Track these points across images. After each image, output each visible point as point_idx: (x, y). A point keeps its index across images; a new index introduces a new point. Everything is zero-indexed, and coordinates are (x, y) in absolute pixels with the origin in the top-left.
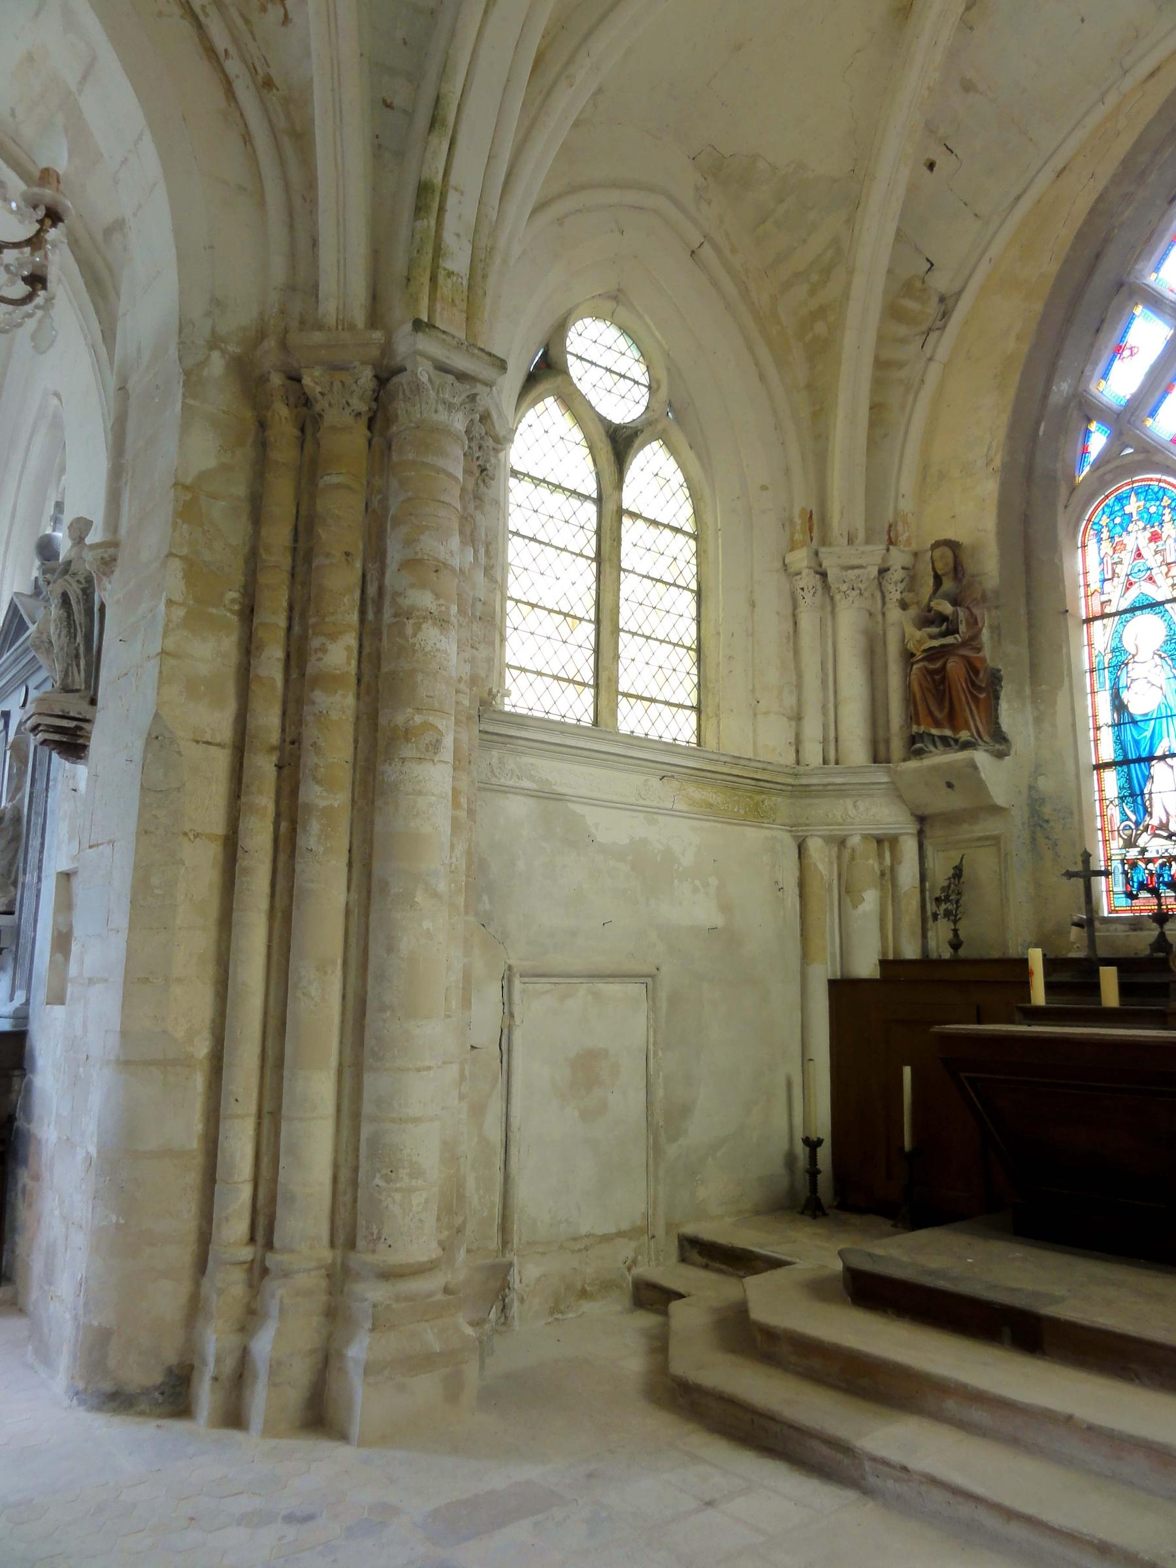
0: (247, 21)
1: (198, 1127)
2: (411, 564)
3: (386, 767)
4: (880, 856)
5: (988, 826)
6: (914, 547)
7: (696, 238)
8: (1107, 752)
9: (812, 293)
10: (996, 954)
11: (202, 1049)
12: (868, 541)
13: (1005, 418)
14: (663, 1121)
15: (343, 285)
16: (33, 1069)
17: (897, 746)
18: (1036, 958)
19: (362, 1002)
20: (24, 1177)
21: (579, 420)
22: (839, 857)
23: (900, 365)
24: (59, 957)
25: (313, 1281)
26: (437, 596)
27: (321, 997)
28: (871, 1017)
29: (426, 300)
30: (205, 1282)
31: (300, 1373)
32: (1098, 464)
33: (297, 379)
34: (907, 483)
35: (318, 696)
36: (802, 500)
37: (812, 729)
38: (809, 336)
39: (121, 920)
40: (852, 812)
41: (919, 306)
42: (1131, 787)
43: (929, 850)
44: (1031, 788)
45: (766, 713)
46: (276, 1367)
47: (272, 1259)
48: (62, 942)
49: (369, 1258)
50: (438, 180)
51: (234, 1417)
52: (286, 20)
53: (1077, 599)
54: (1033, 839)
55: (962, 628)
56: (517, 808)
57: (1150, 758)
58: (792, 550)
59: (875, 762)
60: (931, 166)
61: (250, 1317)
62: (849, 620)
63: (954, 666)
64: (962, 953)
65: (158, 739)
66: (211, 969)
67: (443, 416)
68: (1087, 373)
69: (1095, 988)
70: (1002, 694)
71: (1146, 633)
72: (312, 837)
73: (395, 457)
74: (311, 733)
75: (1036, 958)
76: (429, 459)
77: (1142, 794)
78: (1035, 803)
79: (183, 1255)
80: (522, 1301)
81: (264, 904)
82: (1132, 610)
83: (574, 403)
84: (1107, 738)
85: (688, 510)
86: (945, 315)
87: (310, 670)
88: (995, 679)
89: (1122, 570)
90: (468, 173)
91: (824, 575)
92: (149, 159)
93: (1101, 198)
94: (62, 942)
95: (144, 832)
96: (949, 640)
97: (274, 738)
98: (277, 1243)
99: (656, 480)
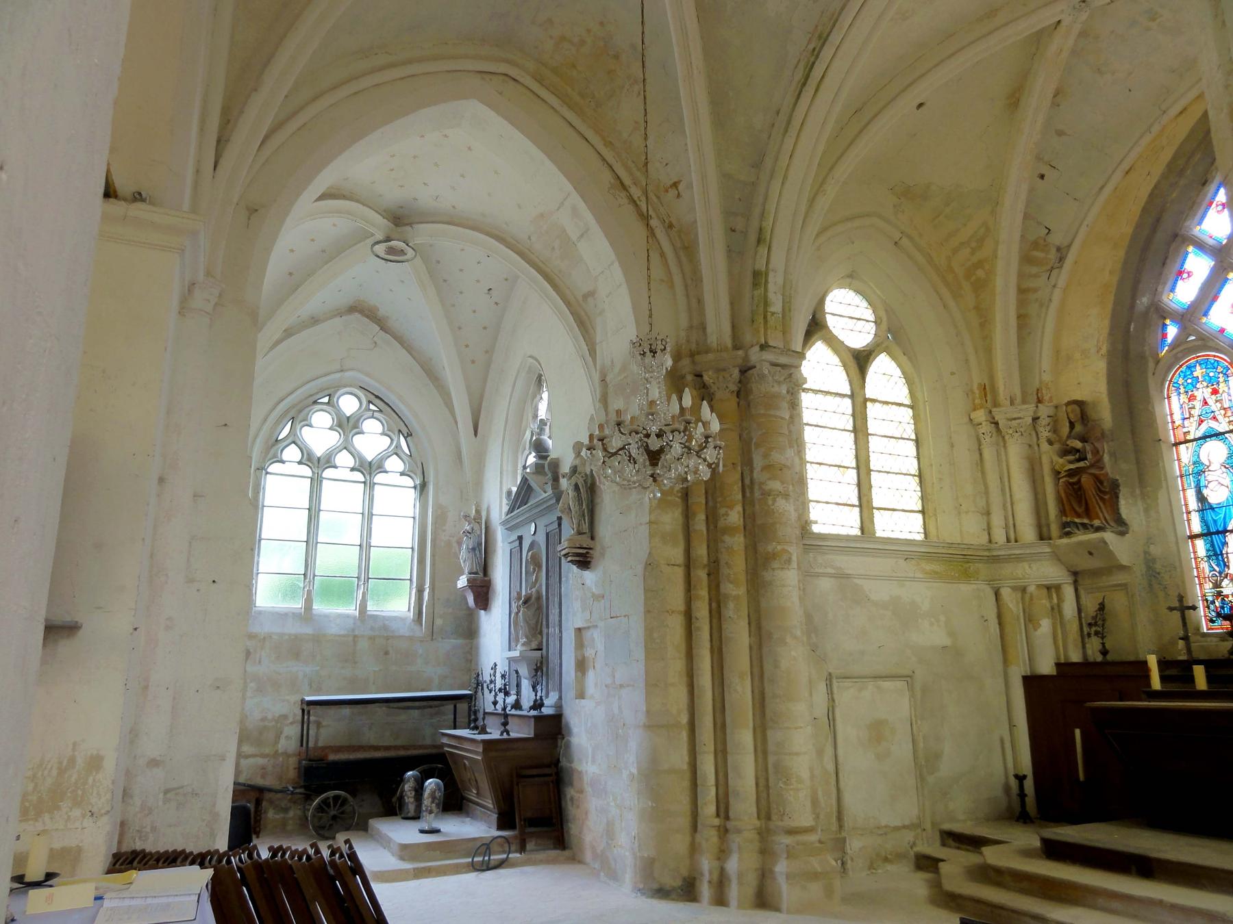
0: (658, 198)
1: (686, 759)
2: (767, 468)
3: (764, 573)
4: (1050, 597)
5: (1120, 578)
6: (1055, 402)
7: (897, 236)
8: (1197, 527)
9: (973, 252)
10: (1132, 658)
11: (684, 719)
12: (1024, 402)
13: (1106, 323)
14: (925, 762)
15: (718, 328)
16: (570, 733)
17: (1055, 530)
18: (1152, 661)
19: (763, 694)
20: (570, 792)
21: (836, 351)
22: (1023, 598)
23: (1035, 290)
24: (579, 674)
25: (752, 835)
26: (783, 483)
27: (741, 691)
28: (1055, 700)
29: (762, 330)
30: (698, 836)
31: (752, 880)
32: (1174, 346)
33: (701, 376)
34: (1046, 364)
35: (727, 538)
36: (977, 379)
37: (997, 521)
38: (973, 278)
39: (640, 654)
40: (1028, 571)
41: (1043, 254)
42: (1214, 550)
43: (1082, 593)
44: (1146, 553)
45: (967, 513)
46: (740, 876)
47: (730, 825)
48: (581, 666)
49: (780, 823)
50: (764, 269)
51: (720, 900)
52: (679, 196)
53: (1168, 431)
54: (1150, 585)
55: (1089, 456)
56: (825, 584)
57: (1225, 531)
58: (974, 410)
59: (1041, 539)
60: (1042, 177)
61: (723, 854)
62: (1015, 452)
63: (1085, 480)
64: (1109, 658)
65: (650, 565)
66: (685, 679)
67: (776, 389)
68: (1159, 289)
69: (1191, 679)
70: (1121, 496)
71: (1215, 452)
72: (730, 610)
73: (753, 411)
74: (724, 557)
75: (1152, 661)
76: (772, 412)
77: (1222, 554)
78: (1150, 563)
79: (684, 822)
80: (852, 860)
81: (708, 645)
82: (1205, 437)
83: (834, 343)
85: (906, 391)
86: (1061, 260)
87: (721, 524)
88: (1115, 486)
89: (1196, 412)
90: (778, 260)
91: (997, 424)
92: (617, 273)
93: (1156, 187)
94: (581, 666)
95: (648, 611)
96: (1081, 464)
97: (705, 560)
98: (731, 814)
99: (885, 376)
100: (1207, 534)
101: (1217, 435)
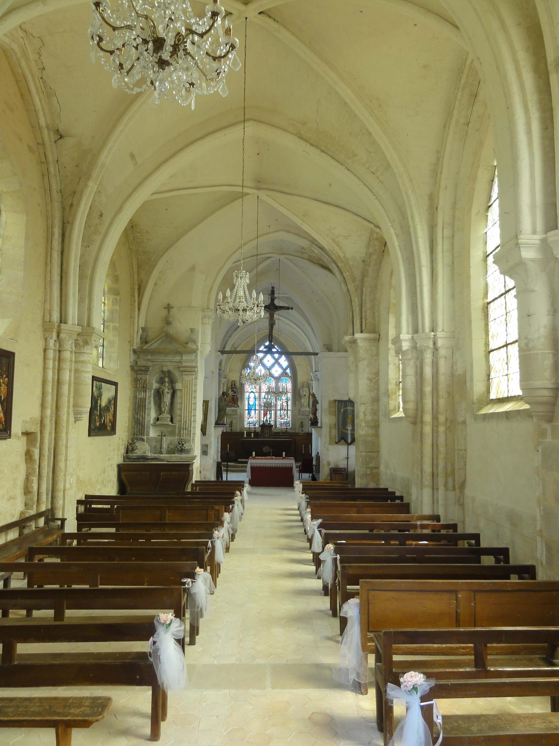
18: (245, 432)
71: (252, 395)
75: (245, 432)
78: (240, 414)
84: (247, 407)
100: (248, 410)
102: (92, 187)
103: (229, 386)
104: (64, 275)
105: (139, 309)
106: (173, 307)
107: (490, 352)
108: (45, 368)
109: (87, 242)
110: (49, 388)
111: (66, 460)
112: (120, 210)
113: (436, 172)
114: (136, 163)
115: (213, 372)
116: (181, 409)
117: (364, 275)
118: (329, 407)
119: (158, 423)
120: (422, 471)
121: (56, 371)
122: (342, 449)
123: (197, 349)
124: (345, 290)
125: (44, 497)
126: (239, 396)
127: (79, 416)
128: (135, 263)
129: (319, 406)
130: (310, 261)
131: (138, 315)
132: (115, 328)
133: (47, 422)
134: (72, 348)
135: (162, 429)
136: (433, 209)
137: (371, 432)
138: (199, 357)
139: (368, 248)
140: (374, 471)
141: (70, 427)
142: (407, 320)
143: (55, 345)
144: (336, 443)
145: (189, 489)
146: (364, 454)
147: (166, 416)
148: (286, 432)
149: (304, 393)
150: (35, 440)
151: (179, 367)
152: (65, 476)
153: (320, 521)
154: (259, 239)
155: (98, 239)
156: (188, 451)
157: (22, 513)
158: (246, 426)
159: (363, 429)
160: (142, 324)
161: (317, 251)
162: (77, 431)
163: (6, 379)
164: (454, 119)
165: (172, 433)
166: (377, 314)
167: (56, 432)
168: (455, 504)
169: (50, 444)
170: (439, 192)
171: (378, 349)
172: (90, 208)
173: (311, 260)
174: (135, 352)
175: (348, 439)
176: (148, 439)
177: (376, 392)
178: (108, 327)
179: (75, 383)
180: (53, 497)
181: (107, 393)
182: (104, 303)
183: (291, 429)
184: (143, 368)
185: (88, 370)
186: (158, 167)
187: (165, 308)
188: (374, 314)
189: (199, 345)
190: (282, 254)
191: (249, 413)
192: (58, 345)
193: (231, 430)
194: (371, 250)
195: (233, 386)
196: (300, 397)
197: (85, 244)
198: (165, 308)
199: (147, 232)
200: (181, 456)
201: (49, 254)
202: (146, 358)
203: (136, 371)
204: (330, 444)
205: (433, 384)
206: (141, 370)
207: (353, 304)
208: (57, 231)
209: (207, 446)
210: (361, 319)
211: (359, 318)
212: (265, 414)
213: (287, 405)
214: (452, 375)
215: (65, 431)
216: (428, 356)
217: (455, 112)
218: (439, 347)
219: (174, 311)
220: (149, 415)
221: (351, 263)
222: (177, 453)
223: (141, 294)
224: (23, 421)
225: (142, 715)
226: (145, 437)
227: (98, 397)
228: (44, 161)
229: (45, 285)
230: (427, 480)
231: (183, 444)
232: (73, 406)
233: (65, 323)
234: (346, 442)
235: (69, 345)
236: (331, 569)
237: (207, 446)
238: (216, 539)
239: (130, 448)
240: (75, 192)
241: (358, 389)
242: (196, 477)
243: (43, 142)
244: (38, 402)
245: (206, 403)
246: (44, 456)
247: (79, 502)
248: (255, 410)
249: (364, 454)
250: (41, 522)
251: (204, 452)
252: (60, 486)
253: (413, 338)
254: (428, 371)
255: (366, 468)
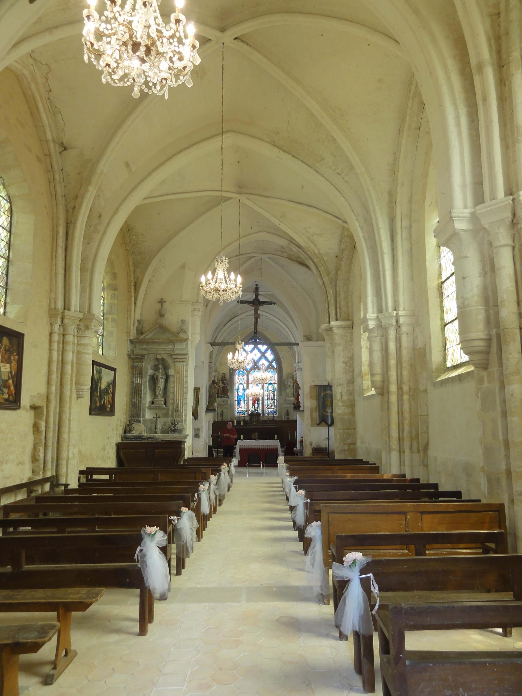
5: (226, 406)
8: (236, 399)
18: (235, 421)
34: (218, 364)
71: (241, 387)
75: (235, 421)
78: (230, 404)
100: (238, 400)
101: (242, 384)
102: (92, 191)
103: (220, 378)
104: (67, 268)
105: (135, 304)
106: (165, 302)
107: (445, 326)
108: (50, 350)
109: (88, 239)
110: (54, 367)
111: (69, 432)
112: (116, 212)
113: (393, 171)
114: (131, 170)
115: (203, 362)
116: (174, 393)
117: (338, 269)
118: (310, 392)
119: (152, 406)
120: (389, 436)
121: (61, 353)
122: (323, 431)
123: (188, 339)
124: (321, 283)
125: (49, 465)
126: (229, 388)
127: (81, 393)
128: (131, 262)
129: (300, 392)
130: (289, 259)
131: (135, 309)
132: (113, 320)
133: (53, 397)
134: (74, 333)
135: (157, 411)
136: (392, 203)
137: (347, 410)
138: (189, 346)
139: (340, 245)
140: (351, 446)
141: (73, 402)
142: (373, 302)
143: (59, 329)
144: (318, 425)
145: (182, 463)
146: (341, 431)
147: (160, 399)
148: (273, 420)
149: (289, 383)
150: (42, 413)
151: (171, 355)
152: (68, 446)
153: (296, 478)
154: (242, 240)
155: (98, 237)
156: (180, 431)
157: (30, 478)
158: (236, 415)
159: (340, 409)
160: (138, 317)
161: (295, 249)
162: (79, 407)
163: (17, 357)
164: (407, 124)
165: (166, 415)
166: (350, 304)
167: (60, 407)
168: (420, 465)
169: (55, 418)
170: (396, 189)
171: (352, 335)
172: (91, 210)
173: (290, 258)
174: (131, 341)
175: (328, 420)
176: (143, 420)
177: (351, 374)
178: (107, 319)
179: (77, 364)
180: (57, 465)
181: (107, 377)
182: (104, 298)
183: (278, 417)
184: (139, 356)
185: (89, 352)
186: (150, 174)
187: (158, 302)
188: (347, 304)
189: (190, 335)
190: (265, 254)
191: (239, 404)
192: (62, 329)
193: (222, 419)
194: (343, 246)
195: (223, 378)
196: (286, 387)
197: (86, 241)
198: (158, 302)
199: (142, 234)
200: (174, 435)
201: (54, 250)
202: (142, 347)
203: (133, 359)
204: (312, 425)
205: (397, 358)
206: (137, 358)
207: (328, 295)
208: (61, 230)
209: (198, 429)
210: (336, 309)
211: (334, 308)
212: (253, 404)
213: (274, 395)
214: (414, 349)
215: (68, 406)
216: (392, 333)
217: (407, 118)
218: (401, 324)
219: (166, 305)
220: (145, 399)
221: (325, 259)
222: (171, 433)
223: (137, 289)
224: (31, 396)
225: (133, 620)
226: (141, 419)
227: (98, 380)
228: (50, 170)
229: (51, 277)
230: (395, 444)
231: (176, 425)
232: (76, 384)
233: (69, 310)
234: (326, 423)
235: (72, 329)
236: (303, 512)
237: (198, 429)
238: (201, 492)
239: (127, 430)
240: (77, 197)
241: (335, 373)
242: (187, 455)
243: (50, 153)
244: (44, 380)
245: (197, 390)
246: (49, 427)
247: (81, 472)
248: (244, 400)
249: (341, 431)
250: (47, 487)
251: (196, 435)
252: (64, 455)
253: (378, 317)
254: (392, 346)
255: (344, 444)
